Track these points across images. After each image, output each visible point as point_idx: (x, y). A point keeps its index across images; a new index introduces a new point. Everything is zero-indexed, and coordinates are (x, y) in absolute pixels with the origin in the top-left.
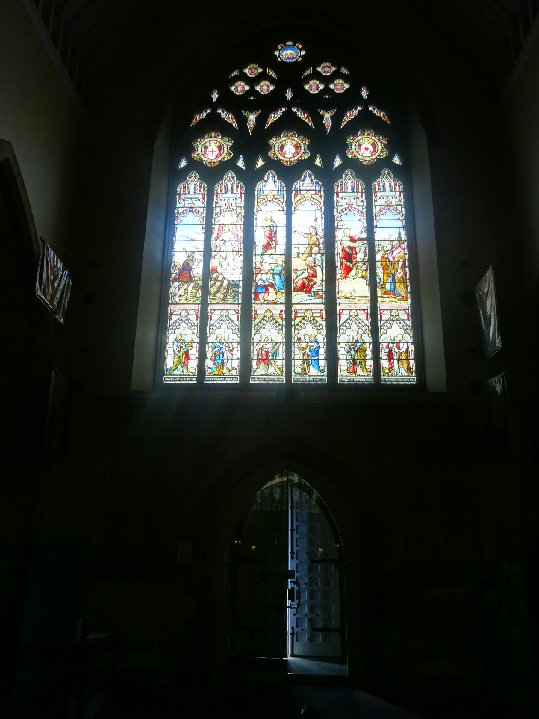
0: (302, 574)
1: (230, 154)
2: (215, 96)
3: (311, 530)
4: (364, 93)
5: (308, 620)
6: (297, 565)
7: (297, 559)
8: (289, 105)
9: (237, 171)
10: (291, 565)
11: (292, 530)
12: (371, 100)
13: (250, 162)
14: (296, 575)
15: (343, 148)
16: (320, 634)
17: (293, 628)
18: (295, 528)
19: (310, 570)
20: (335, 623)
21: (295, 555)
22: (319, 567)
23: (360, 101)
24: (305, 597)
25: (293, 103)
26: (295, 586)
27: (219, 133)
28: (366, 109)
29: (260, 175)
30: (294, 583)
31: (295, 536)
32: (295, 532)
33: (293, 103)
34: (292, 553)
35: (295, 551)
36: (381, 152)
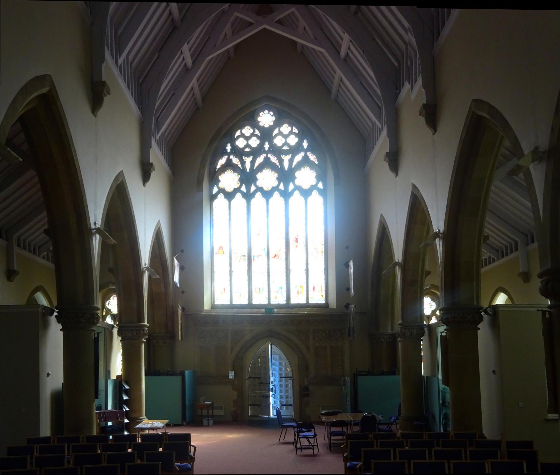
0: (277, 383)
1: (238, 183)
2: (229, 148)
3: (280, 364)
4: (305, 144)
5: (279, 401)
6: (274, 379)
7: (274, 376)
8: (267, 153)
9: (242, 193)
10: (272, 379)
11: (272, 364)
12: (308, 149)
13: (248, 188)
14: (274, 383)
15: (293, 178)
16: (284, 407)
17: (273, 405)
18: (273, 363)
19: (280, 381)
20: (291, 402)
21: (273, 375)
22: (284, 379)
23: (302, 149)
24: (278, 391)
25: (269, 151)
26: (273, 387)
27: (232, 171)
28: (306, 154)
29: (253, 195)
30: (273, 386)
31: (273, 367)
32: (273, 365)
33: (269, 151)
34: (272, 374)
35: (273, 373)
36: (313, 181)
